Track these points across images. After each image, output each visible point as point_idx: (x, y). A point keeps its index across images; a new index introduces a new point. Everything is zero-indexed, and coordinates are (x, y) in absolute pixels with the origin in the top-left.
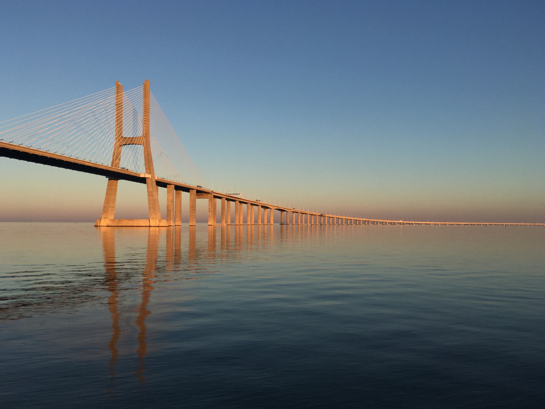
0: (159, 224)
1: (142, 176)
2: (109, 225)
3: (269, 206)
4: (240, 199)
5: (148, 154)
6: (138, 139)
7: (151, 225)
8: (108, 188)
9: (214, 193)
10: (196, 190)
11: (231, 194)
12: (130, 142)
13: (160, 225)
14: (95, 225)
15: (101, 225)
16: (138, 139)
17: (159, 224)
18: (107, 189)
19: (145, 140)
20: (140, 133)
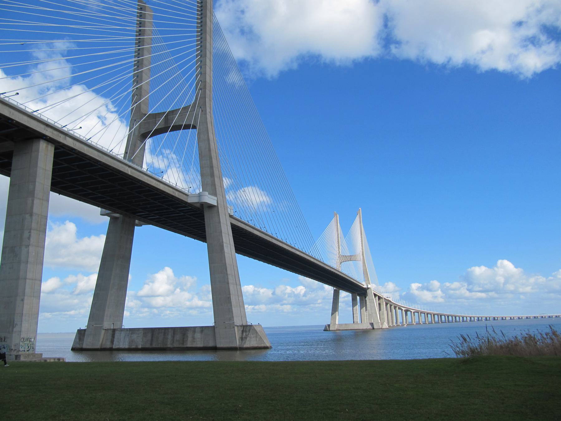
0: (382, 326)
1: (365, 286)
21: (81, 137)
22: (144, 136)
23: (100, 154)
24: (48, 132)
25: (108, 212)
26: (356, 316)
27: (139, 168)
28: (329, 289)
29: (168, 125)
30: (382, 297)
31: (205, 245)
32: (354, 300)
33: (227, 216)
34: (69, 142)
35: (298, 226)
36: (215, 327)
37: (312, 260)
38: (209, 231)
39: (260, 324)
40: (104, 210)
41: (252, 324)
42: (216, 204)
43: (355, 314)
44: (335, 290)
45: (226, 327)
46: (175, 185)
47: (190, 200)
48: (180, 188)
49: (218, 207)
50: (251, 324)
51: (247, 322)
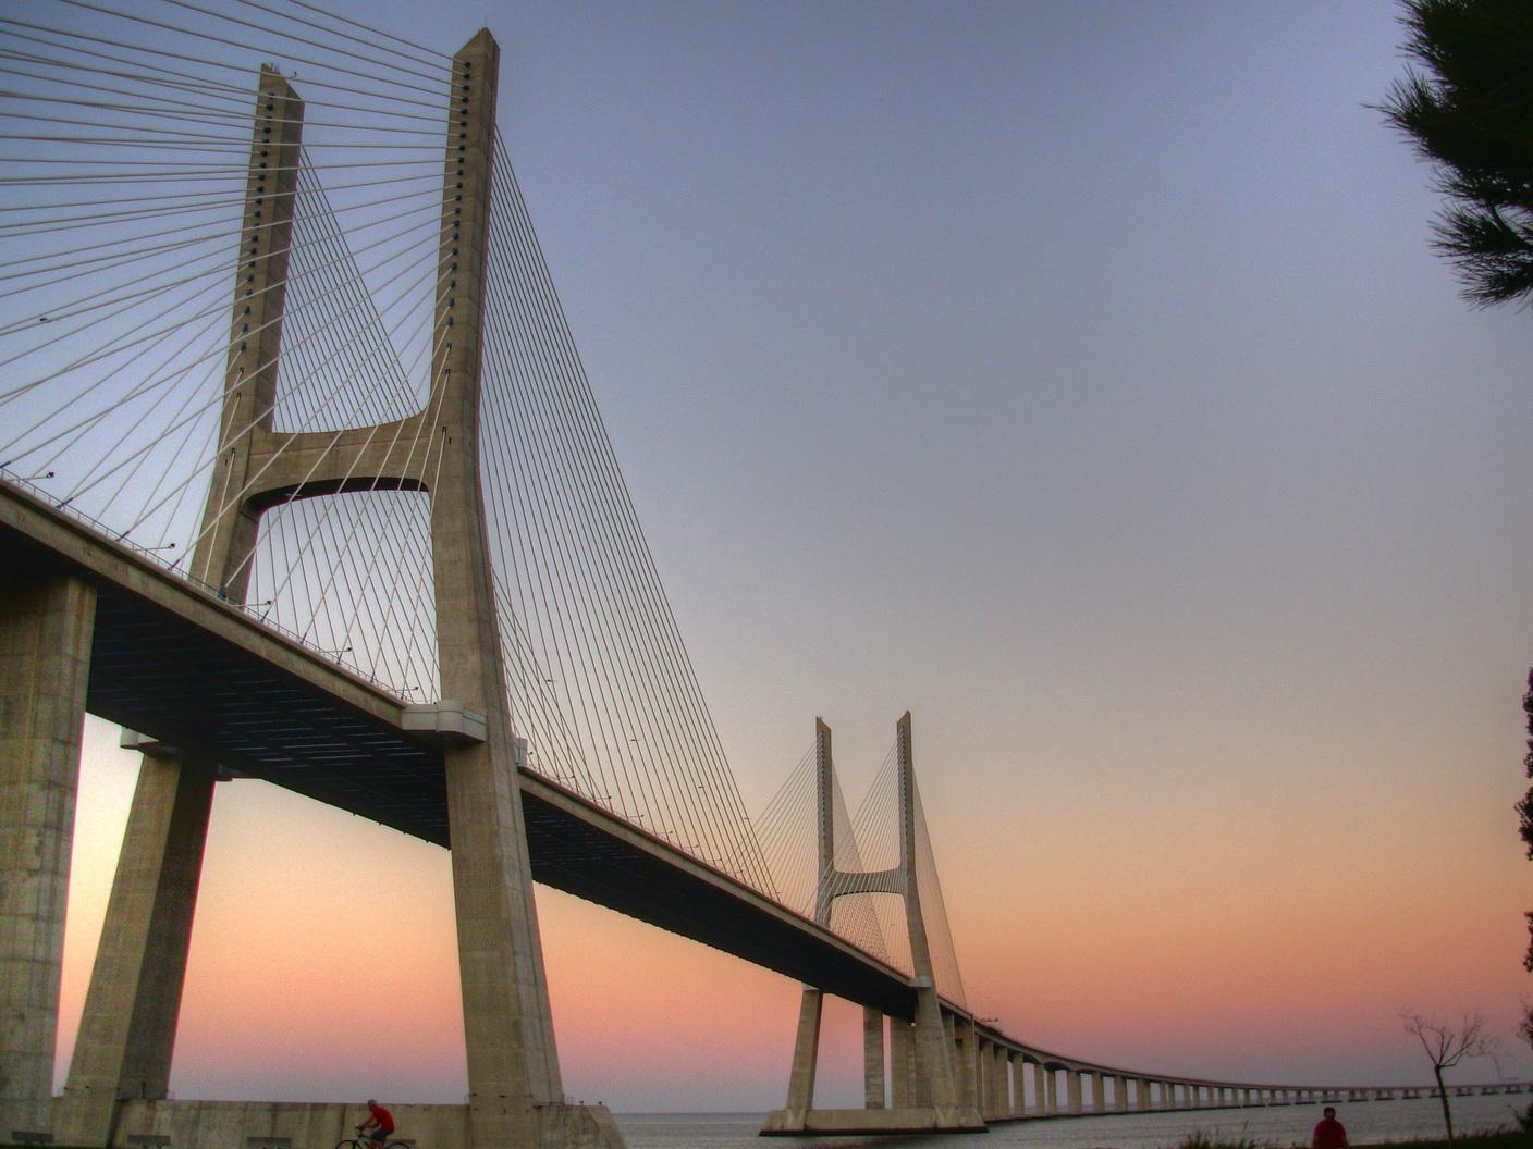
1: (911, 985)
3: (1038, 1057)
4: (997, 1034)
9: (978, 1025)
11: (989, 1020)
12: (864, 884)
19: (907, 879)
21: (141, 553)
22: (257, 505)
23: (199, 607)
24: (96, 561)
25: (144, 739)
26: (876, 1085)
27: (234, 607)
28: (788, 992)
29: (339, 477)
30: (969, 1018)
31: (438, 860)
32: (872, 1027)
33: (513, 769)
34: (134, 580)
35: (705, 784)
36: (472, 1107)
37: (744, 896)
38: (457, 817)
39: (604, 1104)
40: (130, 732)
41: (585, 1104)
42: (483, 738)
43: (872, 1076)
44: (806, 992)
45: (505, 1111)
46: (369, 679)
47: (408, 723)
48: (384, 688)
49: (489, 746)
50: (582, 1102)
51: (563, 1096)
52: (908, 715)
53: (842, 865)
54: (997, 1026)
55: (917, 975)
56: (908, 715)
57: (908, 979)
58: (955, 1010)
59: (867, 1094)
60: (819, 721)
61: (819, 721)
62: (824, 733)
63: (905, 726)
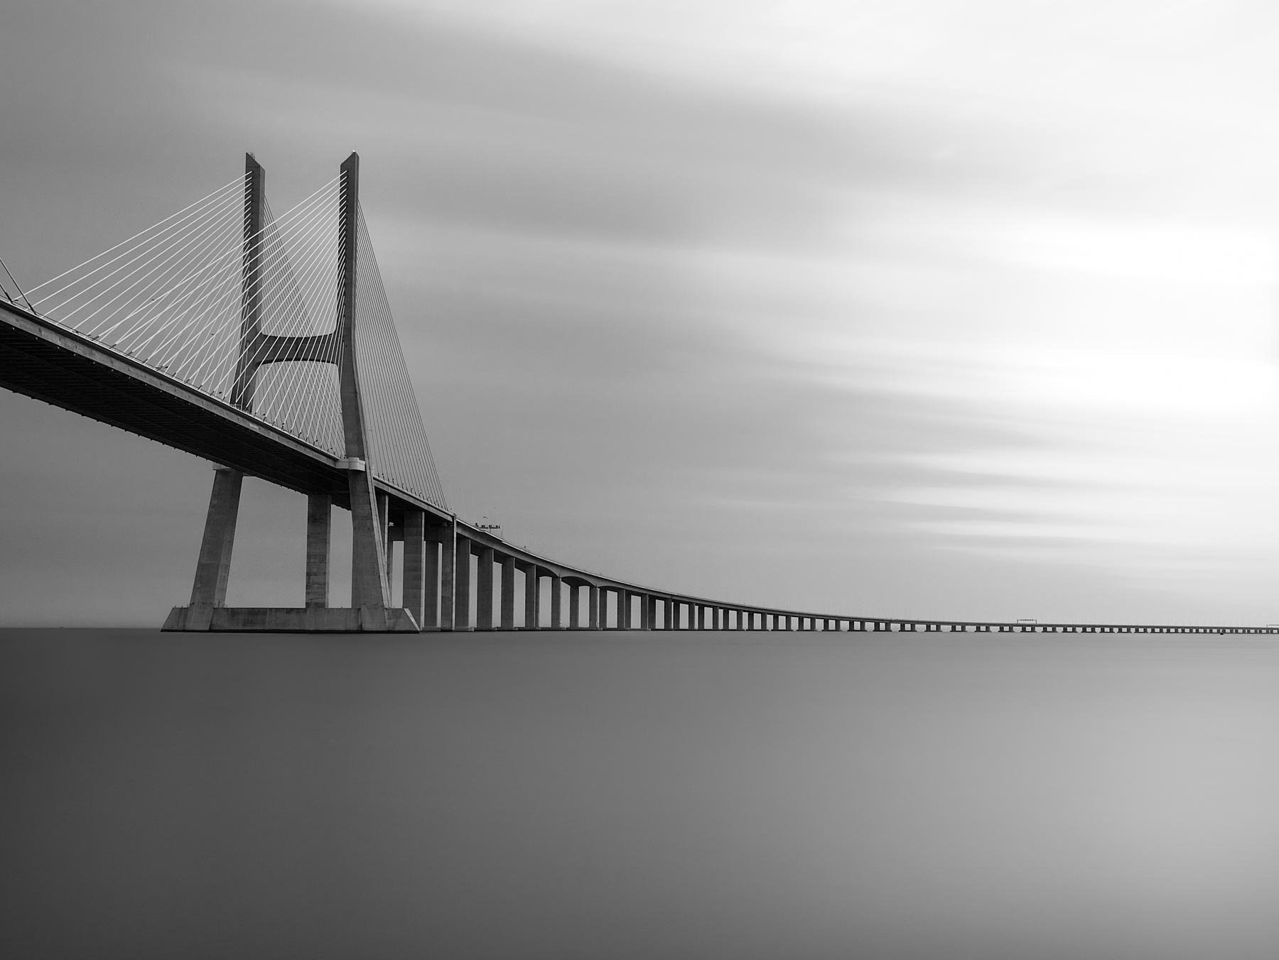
0: (395, 624)
1: (340, 466)
2: (218, 628)
4: (499, 542)
5: (356, 392)
6: (318, 342)
7: (367, 627)
8: (216, 502)
10: (423, 513)
11: (483, 526)
13: (397, 629)
14: (166, 628)
15: (187, 629)
16: (318, 342)
17: (395, 624)
18: (212, 506)
20: (324, 324)
30: (450, 519)
32: (318, 521)
43: (315, 574)
44: (219, 472)
52: (354, 157)
53: (269, 327)
54: (494, 533)
55: (347, 456)
56: (354, 157)
57: (335, 460)
58: (426, 507)
59: (308, 593)
60: (250, 159)
61: (250, 159)
62: (254, 172)
63: (350, 169)
